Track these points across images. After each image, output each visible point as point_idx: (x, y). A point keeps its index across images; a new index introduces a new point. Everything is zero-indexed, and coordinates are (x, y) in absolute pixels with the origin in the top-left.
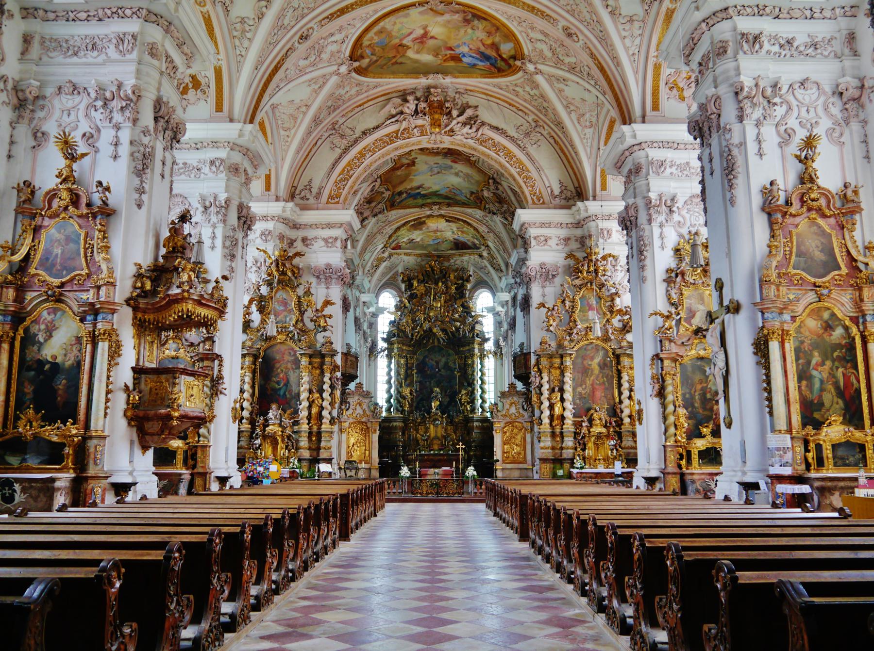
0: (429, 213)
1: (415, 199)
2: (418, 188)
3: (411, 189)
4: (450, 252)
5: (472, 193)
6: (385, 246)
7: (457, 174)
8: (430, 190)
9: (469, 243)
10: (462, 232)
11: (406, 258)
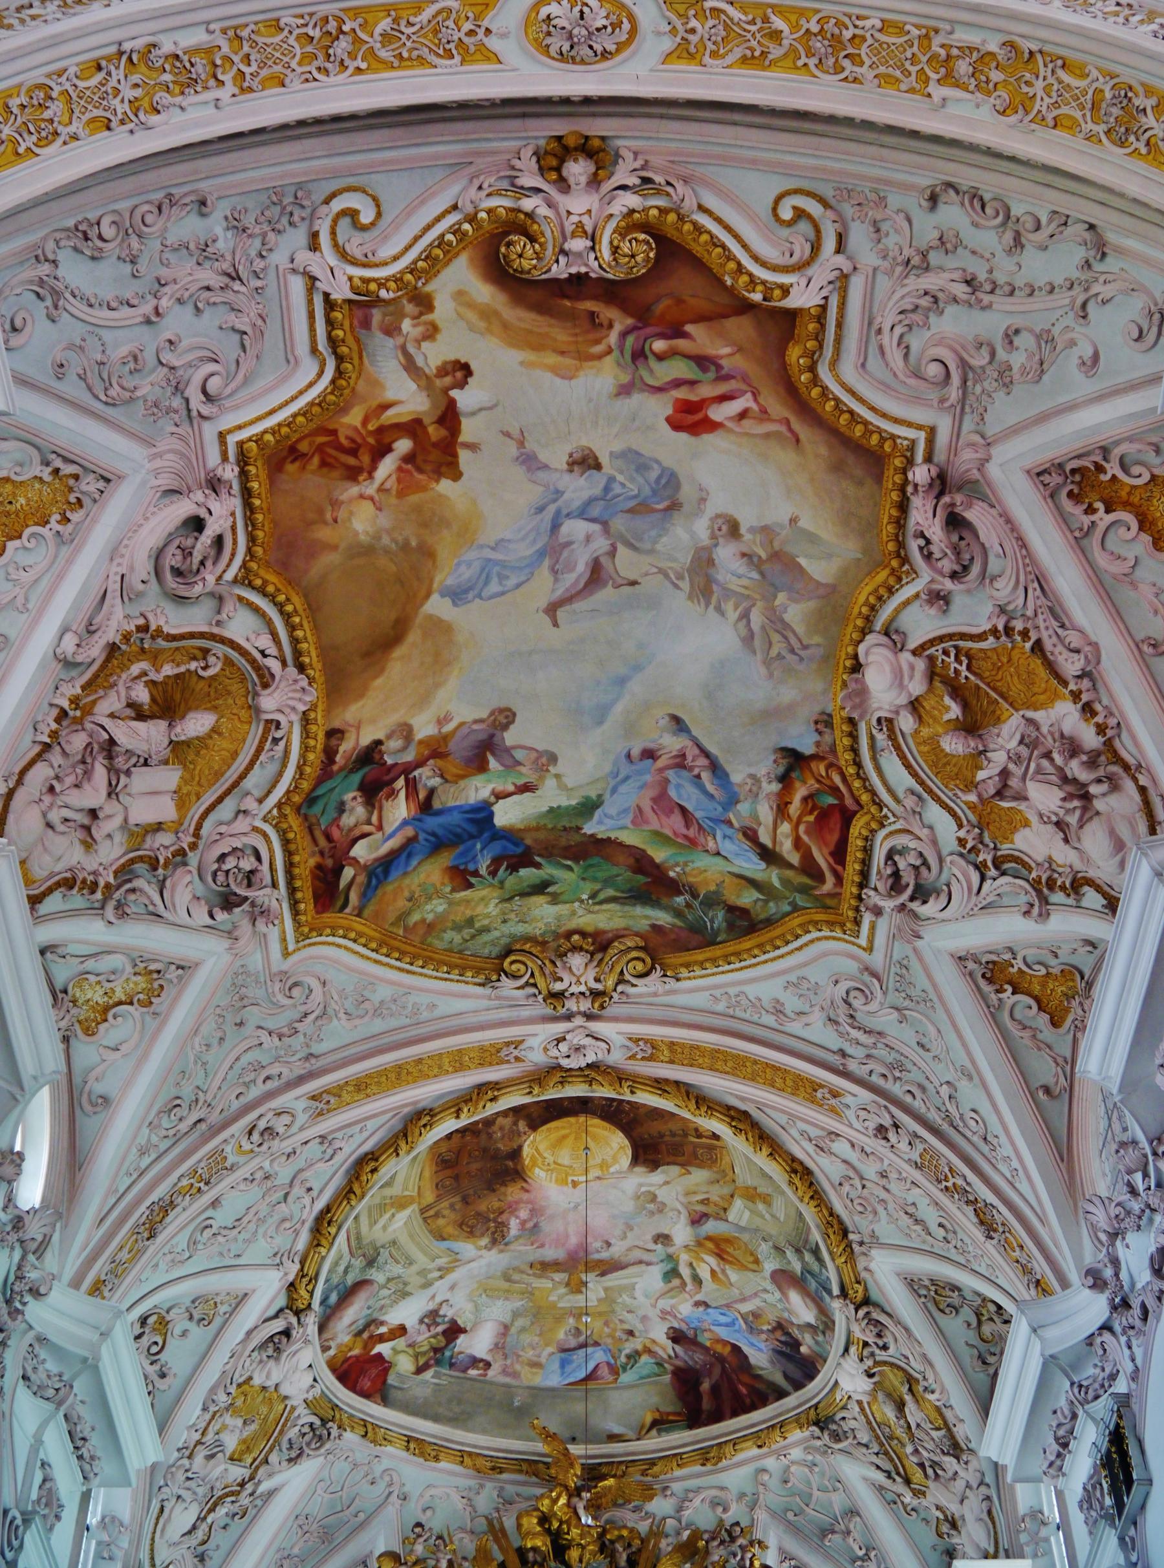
0: (538, 1042)
1: (462, 877)
2: (484, 750)
3: (436, 750)
4: (654, 1443)
5: (794, 762)
6: (294, 1307)
7: (702, 579)
8: (551, 796)
9: (760, 1355)
10: (721, 1248)
11: (414, 1474)
